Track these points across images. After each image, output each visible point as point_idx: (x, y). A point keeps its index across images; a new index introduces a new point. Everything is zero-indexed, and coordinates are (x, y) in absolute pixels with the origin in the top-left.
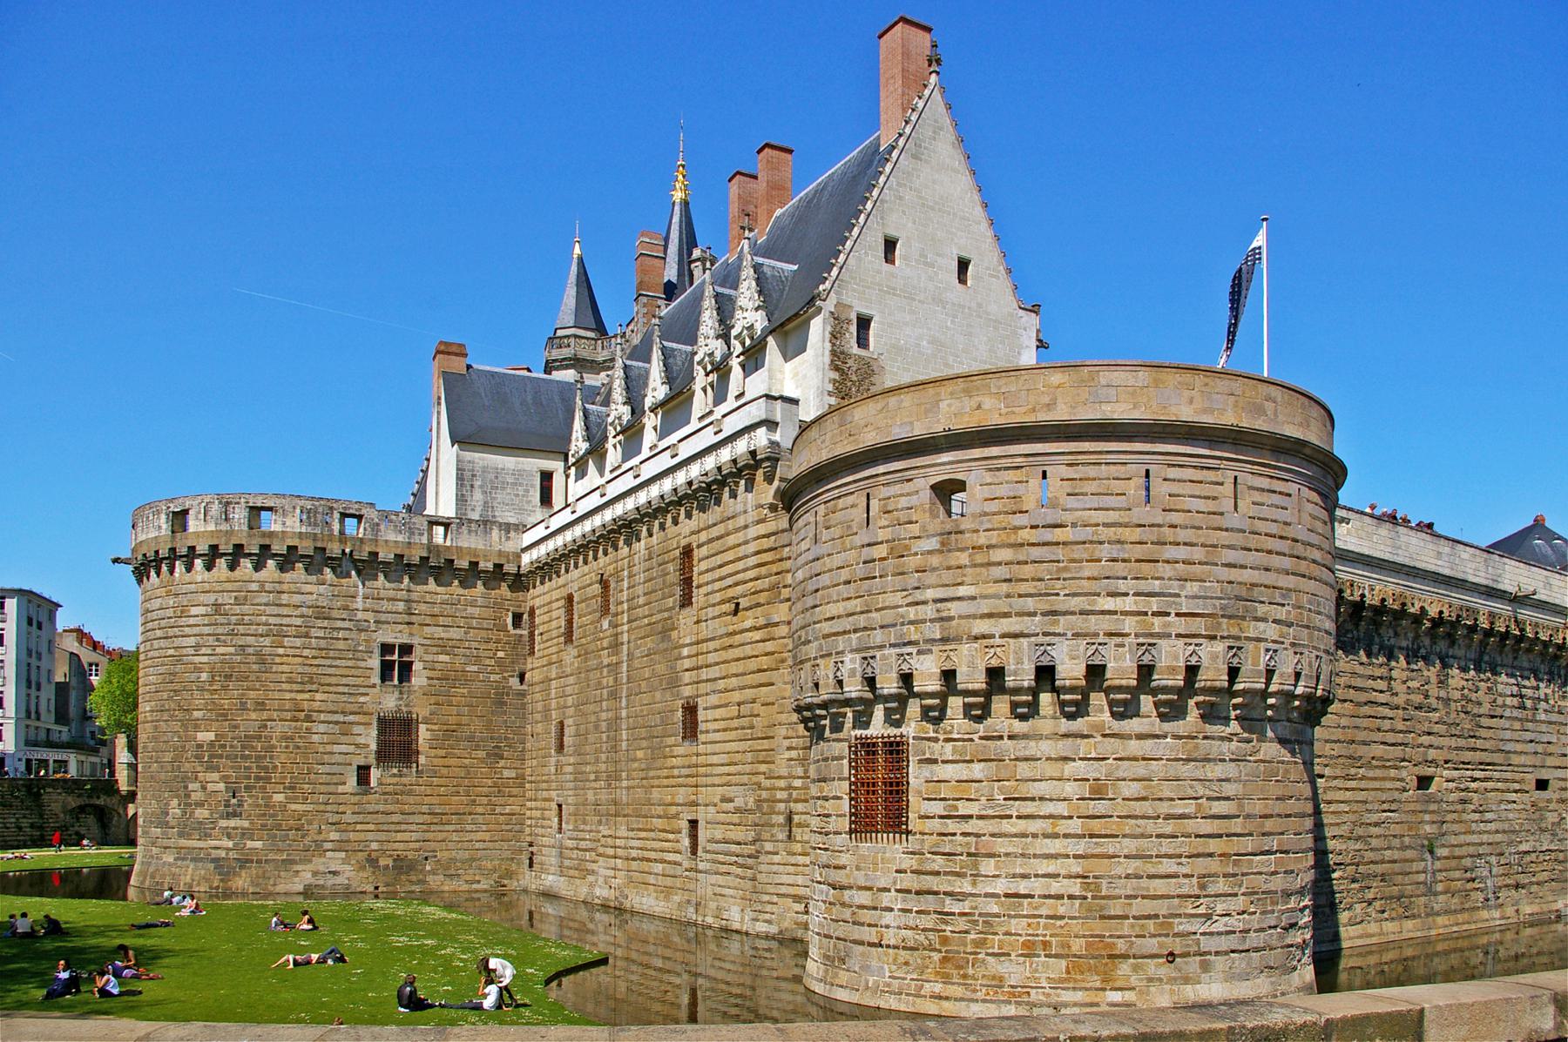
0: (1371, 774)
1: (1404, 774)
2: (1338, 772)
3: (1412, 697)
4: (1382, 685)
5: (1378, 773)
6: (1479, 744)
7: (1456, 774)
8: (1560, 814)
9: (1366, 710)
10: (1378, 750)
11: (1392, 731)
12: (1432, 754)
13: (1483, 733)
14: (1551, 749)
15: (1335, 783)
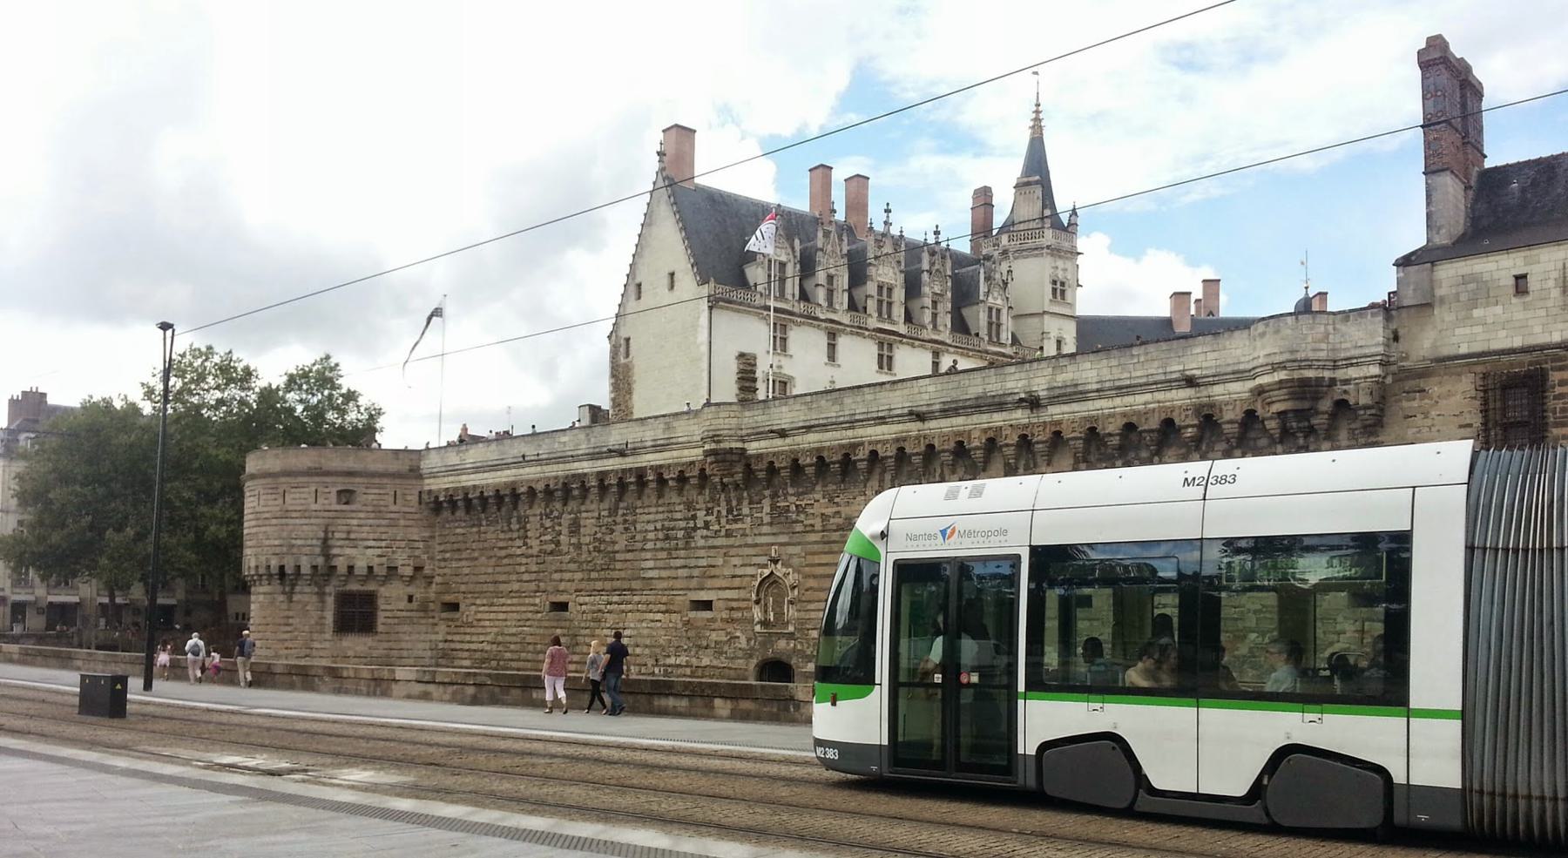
0: (509, 602)
1: (537, 601)
2: (485, 602)
3: (544, 547)
4: (519, 543)
5: (515, 601)
6: (615, 574)
7: (587, 599)
8: (728, 634)
9: (505, 561)
10: (516, 586)
11: (527, 572)
12: (562, 586)
13: (619, 565)
14: (713, 572)
15: (482, 609)
